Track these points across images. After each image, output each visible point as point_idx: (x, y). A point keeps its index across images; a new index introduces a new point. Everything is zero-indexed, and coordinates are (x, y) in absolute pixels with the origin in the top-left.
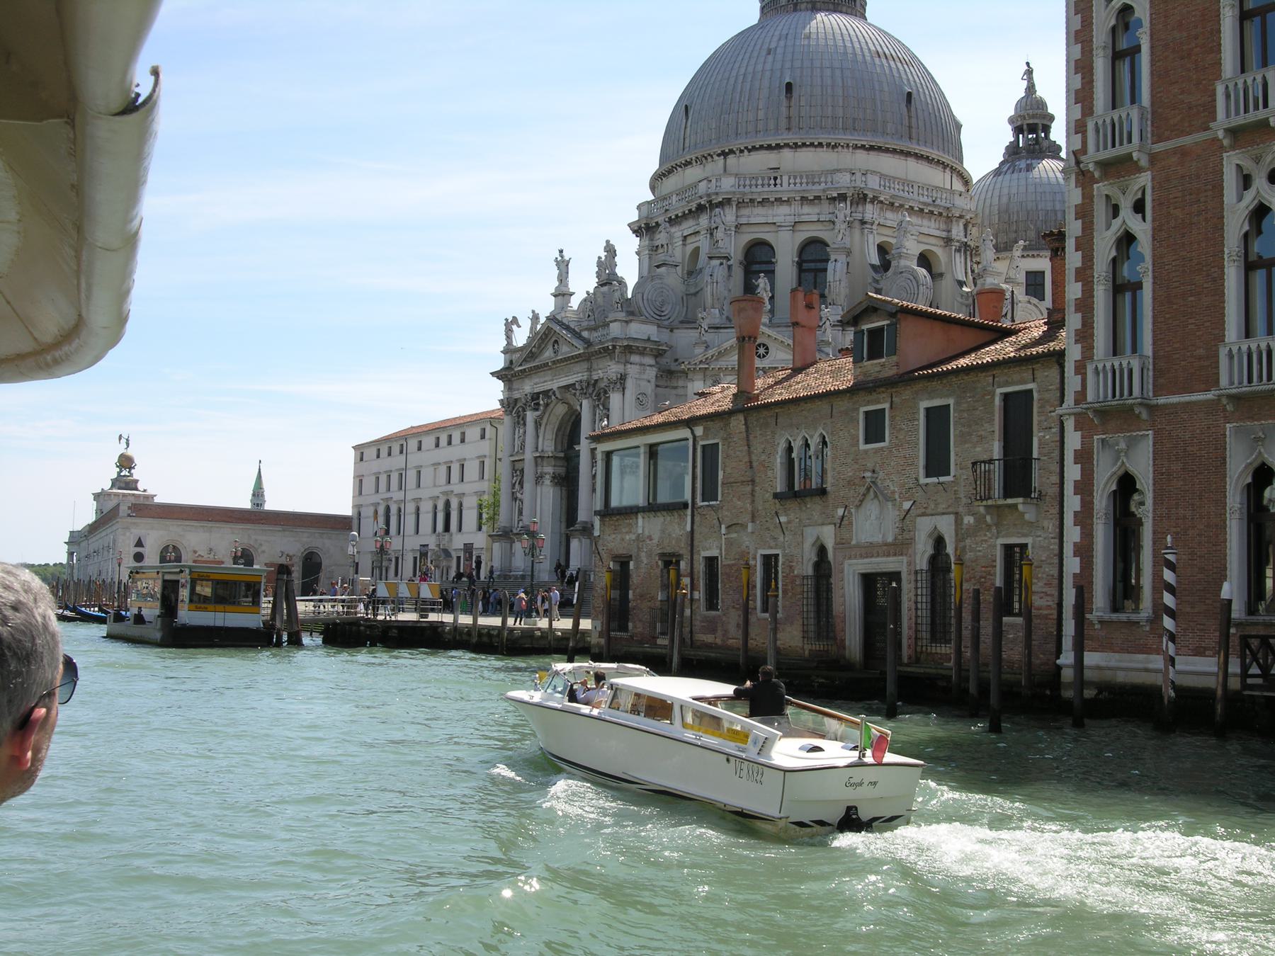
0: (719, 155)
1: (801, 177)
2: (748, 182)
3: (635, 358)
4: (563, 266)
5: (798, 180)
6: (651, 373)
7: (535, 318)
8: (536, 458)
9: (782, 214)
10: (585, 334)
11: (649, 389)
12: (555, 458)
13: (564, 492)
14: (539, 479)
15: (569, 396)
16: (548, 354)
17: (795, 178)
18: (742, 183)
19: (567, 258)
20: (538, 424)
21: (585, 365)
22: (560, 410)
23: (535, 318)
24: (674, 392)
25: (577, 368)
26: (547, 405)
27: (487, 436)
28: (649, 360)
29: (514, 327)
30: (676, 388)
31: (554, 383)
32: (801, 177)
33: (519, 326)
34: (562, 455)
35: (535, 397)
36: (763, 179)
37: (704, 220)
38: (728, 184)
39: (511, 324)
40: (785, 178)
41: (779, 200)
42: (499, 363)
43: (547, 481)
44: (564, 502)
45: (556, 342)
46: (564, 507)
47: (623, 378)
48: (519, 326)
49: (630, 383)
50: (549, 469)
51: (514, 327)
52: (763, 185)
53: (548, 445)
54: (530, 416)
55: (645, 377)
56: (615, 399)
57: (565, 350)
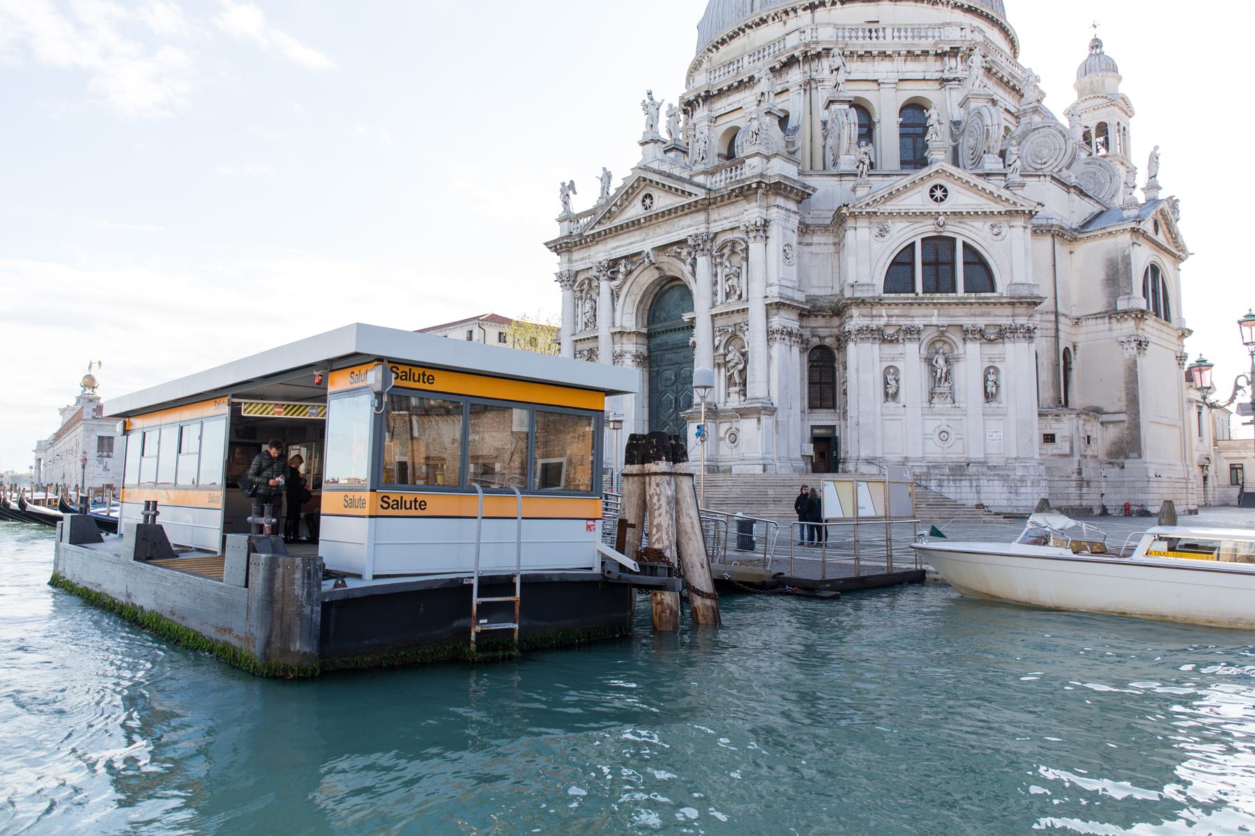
0: (804, 9)
1: (906, 31)
2: (847, 34)
3: (780, 201)
4: (652, 109)
5: (903, 34)
6: (794, 221)
7: (607, 177)
8: (613, 334)
9: (881, 69)
10: (700, 179)
11: (794, 239)
12: (638, 334)
13: (646, 375)
14: (617, 357)
15: (663, 258)
16: (635, 210)
17: (899, 30)
18: (840, 34)
19: (657, 99)
20: (614, 295)
21: (701, 217)
22: (647, 277)
23: (607, 177)
24: (808, 249)
25: (687, 221)
26: (629, 273)
27: (475, 336)
28: (792, 206)
29: (571, 193)
30: (811, 244)
31: (643, 242)
32: (906, 31)
33: (575, 193)
34: (645, 330)
35: (615, 262)
36: (864, 30)
37: (795, 76)
38: (826, 35)
39: (568, 189)
40: (889, 31)
41: (883, 55)
42: (555, 232)
43: (628, 361)
44: (646, 385)
45: (649, 196)
46: (646, 390)
47: (766, 224)
48: (575, 193)
49: (773, 231)
50: (631, 347)
51: (571, 193)
52: (864, 38)
53: (628, 318)
54: (605, 286)
55: (789, 225)
56: (756, 248)
57: (662, 201)
